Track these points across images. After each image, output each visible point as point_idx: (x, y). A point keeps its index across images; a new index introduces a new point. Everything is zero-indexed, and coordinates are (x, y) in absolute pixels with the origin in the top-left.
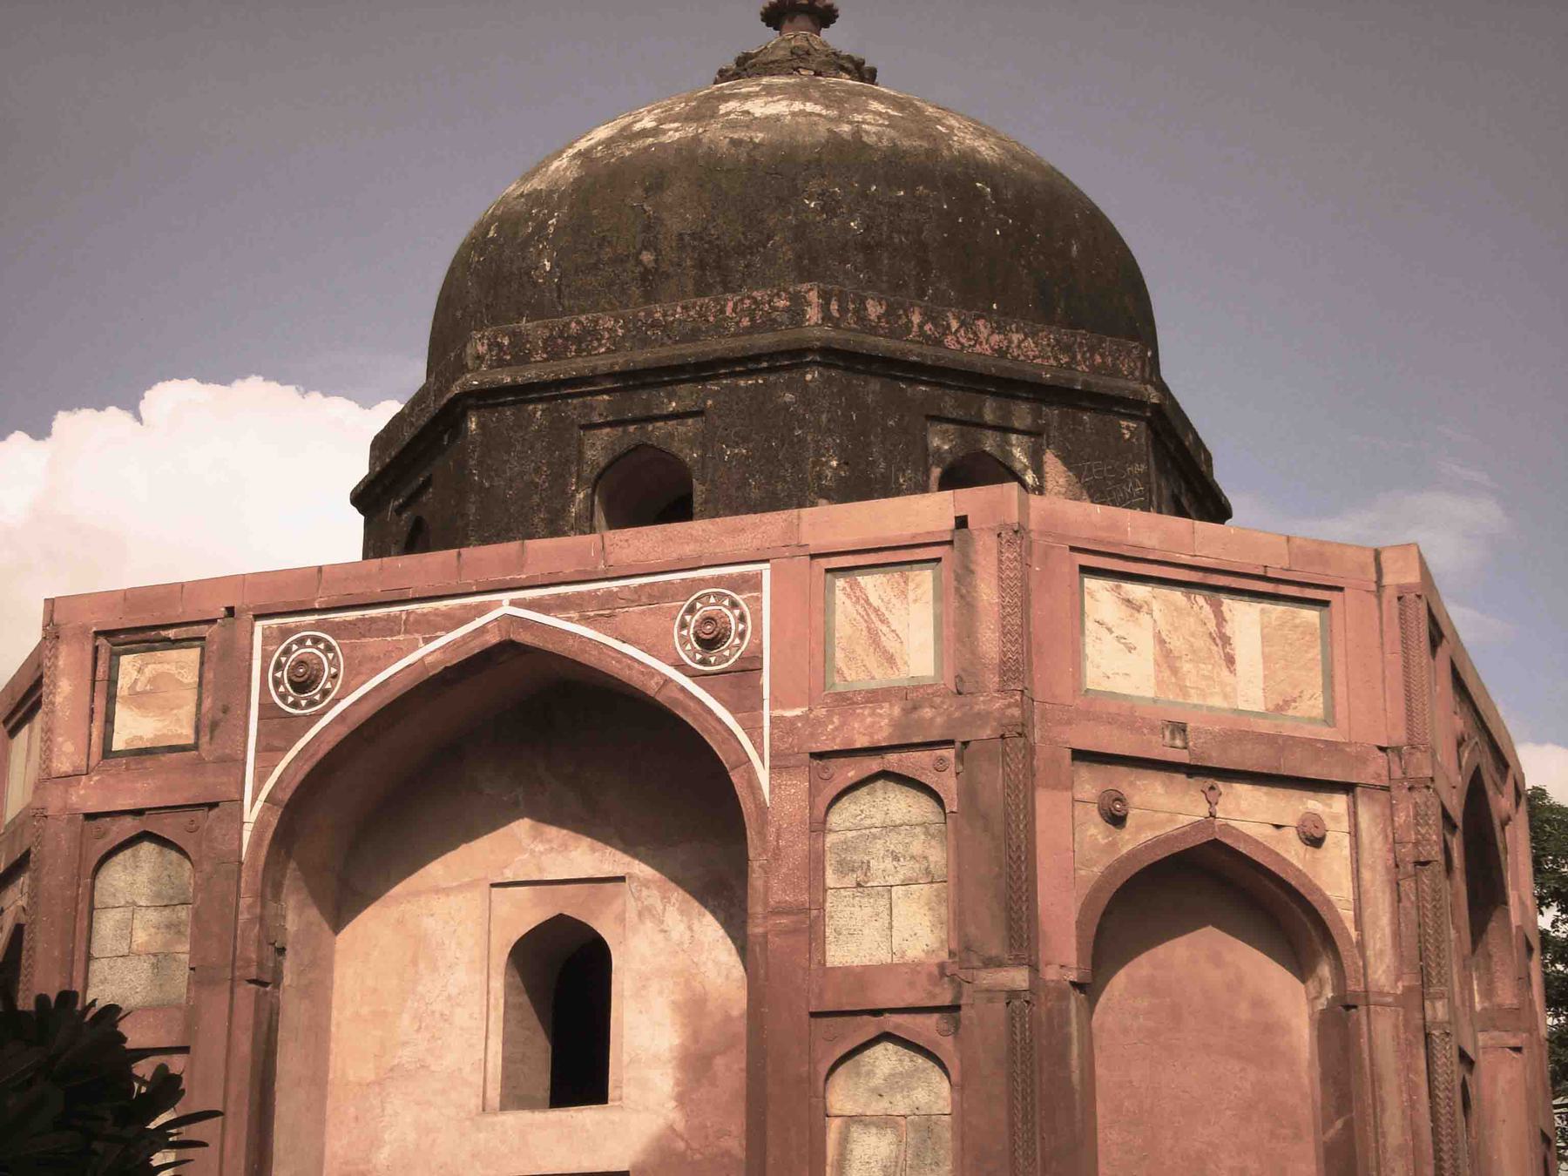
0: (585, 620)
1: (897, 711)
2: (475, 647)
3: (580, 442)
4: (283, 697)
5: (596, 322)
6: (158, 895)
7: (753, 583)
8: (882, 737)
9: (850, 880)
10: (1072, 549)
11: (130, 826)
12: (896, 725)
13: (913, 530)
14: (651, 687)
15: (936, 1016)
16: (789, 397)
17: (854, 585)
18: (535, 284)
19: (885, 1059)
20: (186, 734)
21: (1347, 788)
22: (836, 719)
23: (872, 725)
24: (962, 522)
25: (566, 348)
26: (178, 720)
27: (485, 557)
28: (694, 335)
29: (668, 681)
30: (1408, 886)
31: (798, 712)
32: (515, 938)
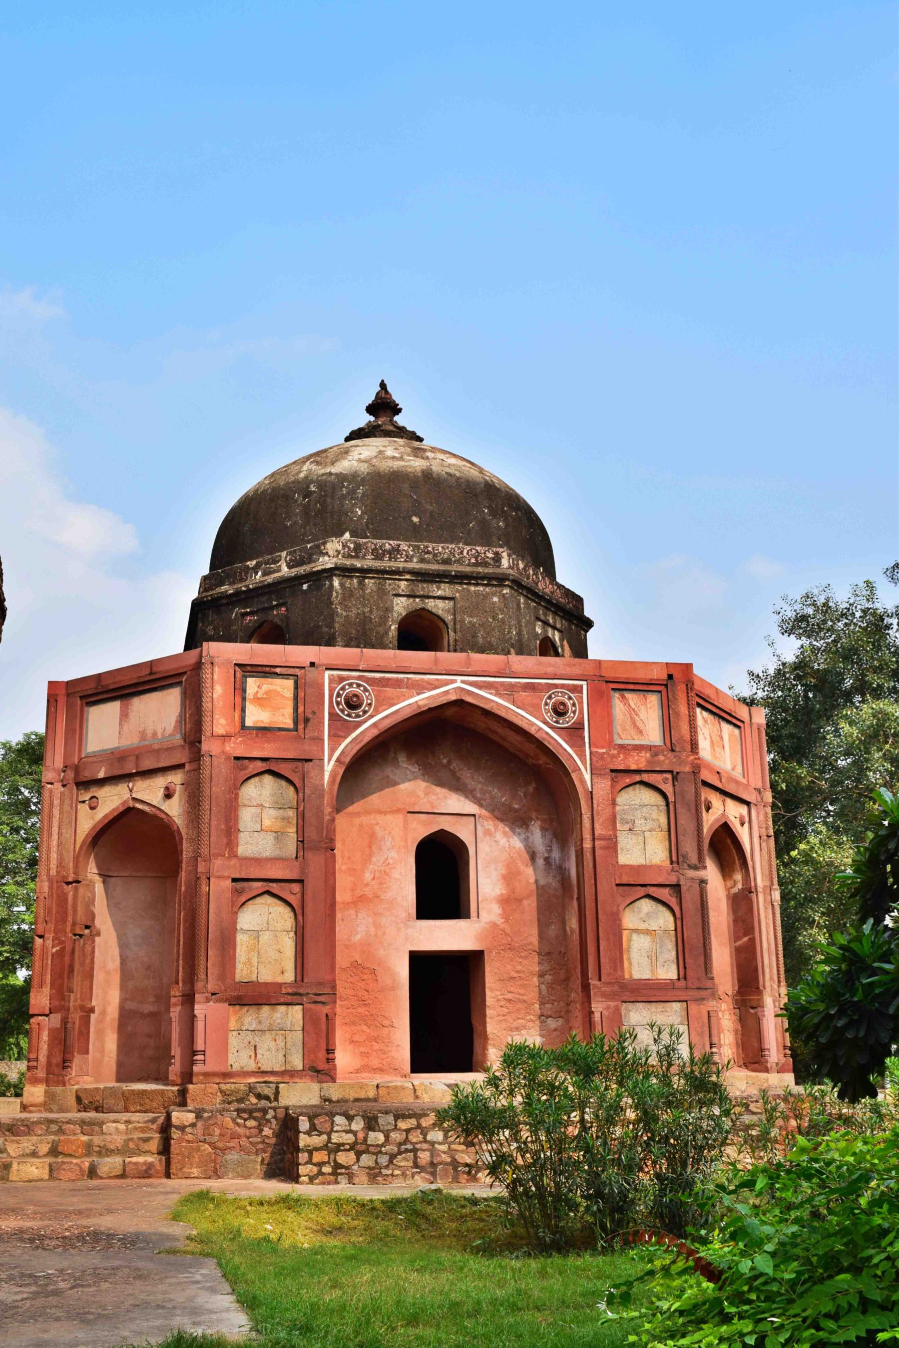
0: (498, 694)
1: (648, 755)
2: (444, 700)
3: (392, 601)
4: (342, 711)
5: (399, 546)
6: (277, 802)
7: (577, 690)
8: (642, 766)
9: (627, 827)
10: (697, 695)
11: (260, 766)
12: (649, 762)
13: (625, 676)
14: (532, 731)
15: (668, 889)
16: (495, 599)
17: (623, 697)
18: (351, 519)
19: (646, 905)
20: (288, 723)
21: (748, 803)
22: (621, 756)
23: (638, 760)
24: (670, 677)
25: (384, 555)
26: (283, 715)
27: (446, 657)
28: (446, 562)
29: (540, 729)
30: (764, 845)
31: (604, 751)
32: (420, 839)
